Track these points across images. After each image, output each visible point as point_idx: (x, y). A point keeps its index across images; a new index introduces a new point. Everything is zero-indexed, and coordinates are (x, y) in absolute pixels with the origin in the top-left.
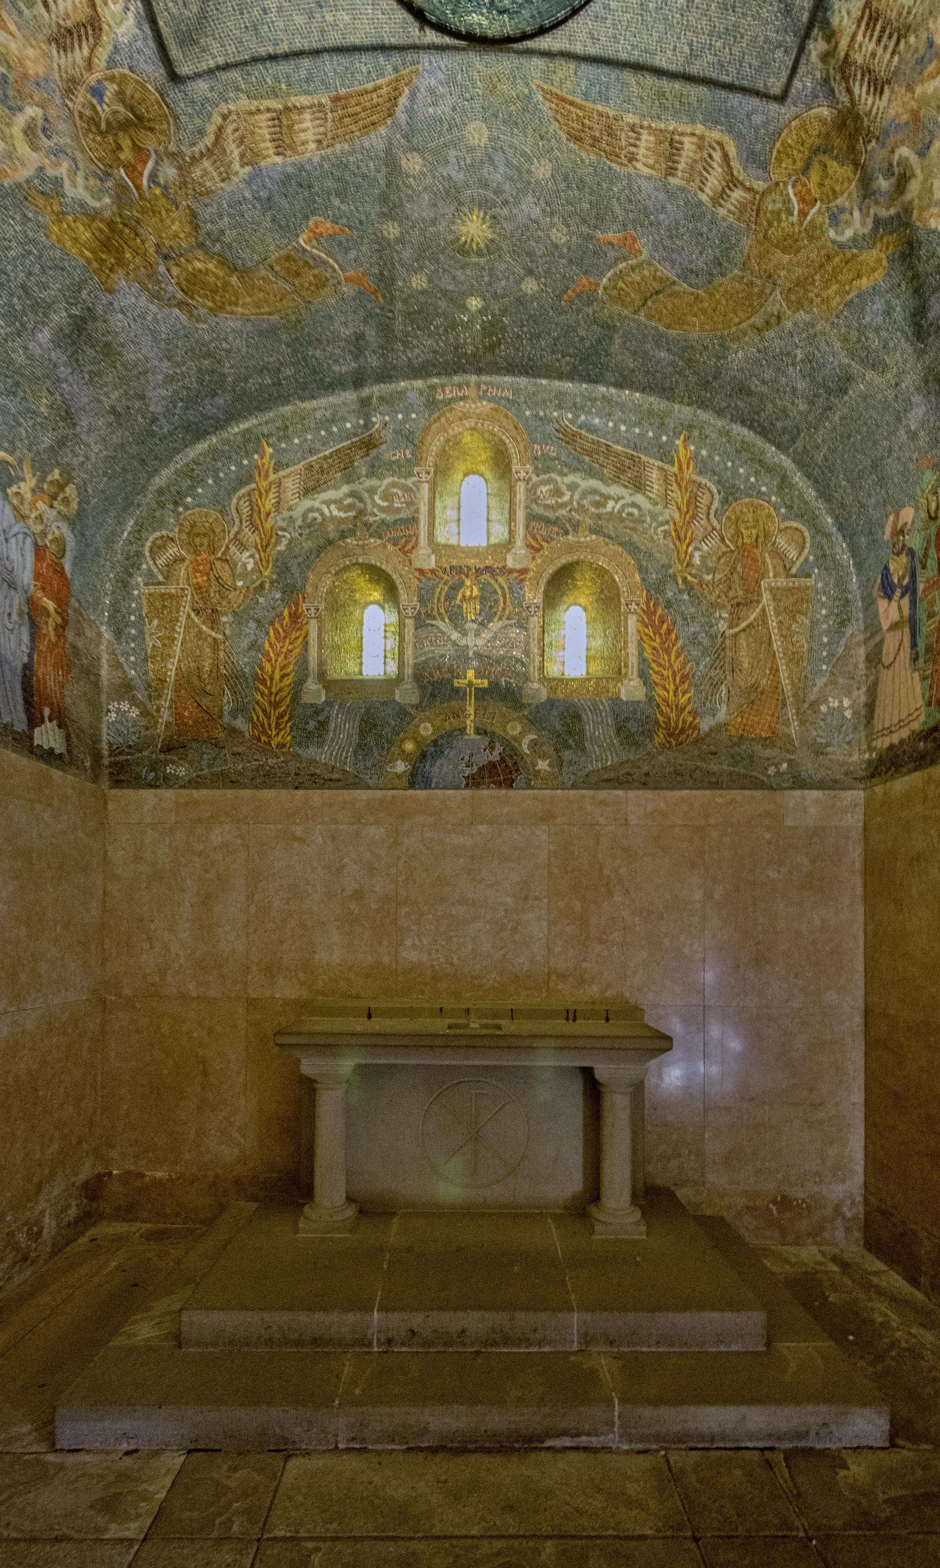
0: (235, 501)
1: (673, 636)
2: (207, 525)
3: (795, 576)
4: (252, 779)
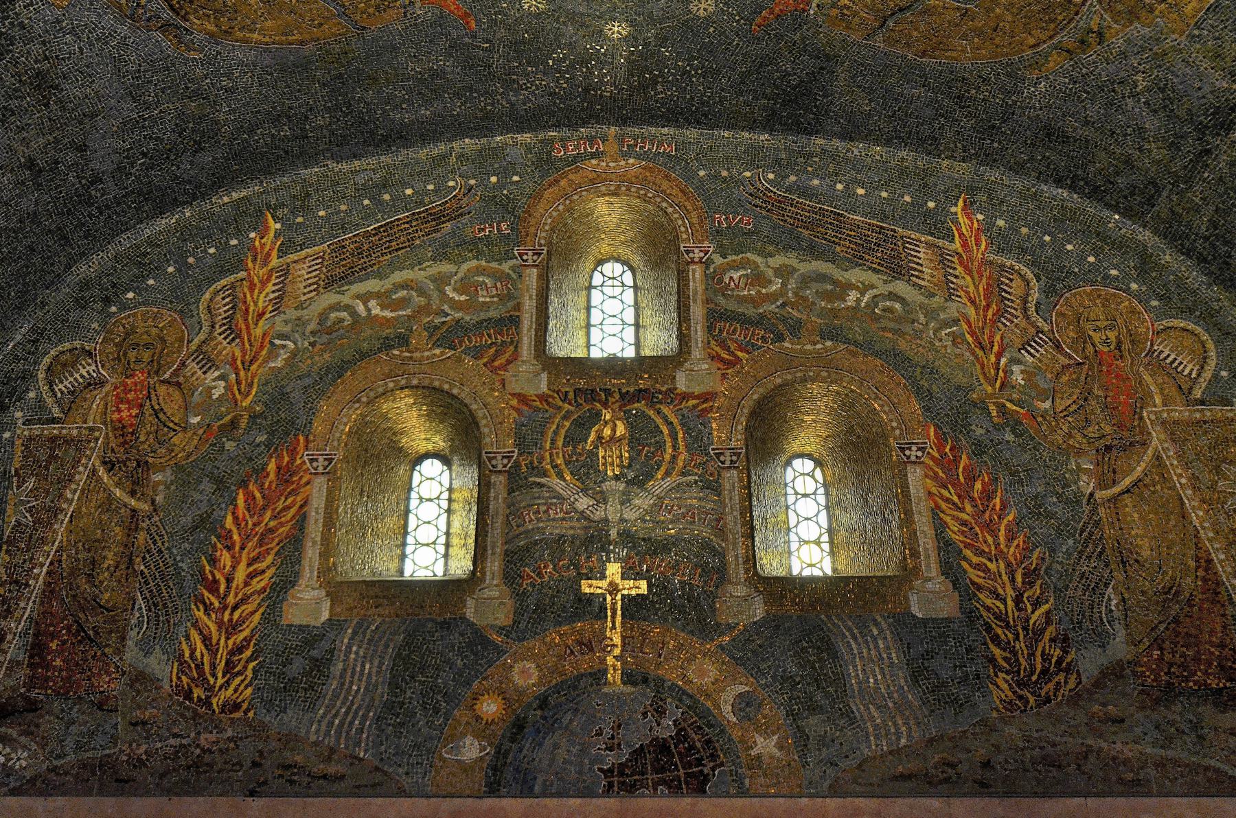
0: (207, 296)
2: (154, 331)
4: (162, 776)
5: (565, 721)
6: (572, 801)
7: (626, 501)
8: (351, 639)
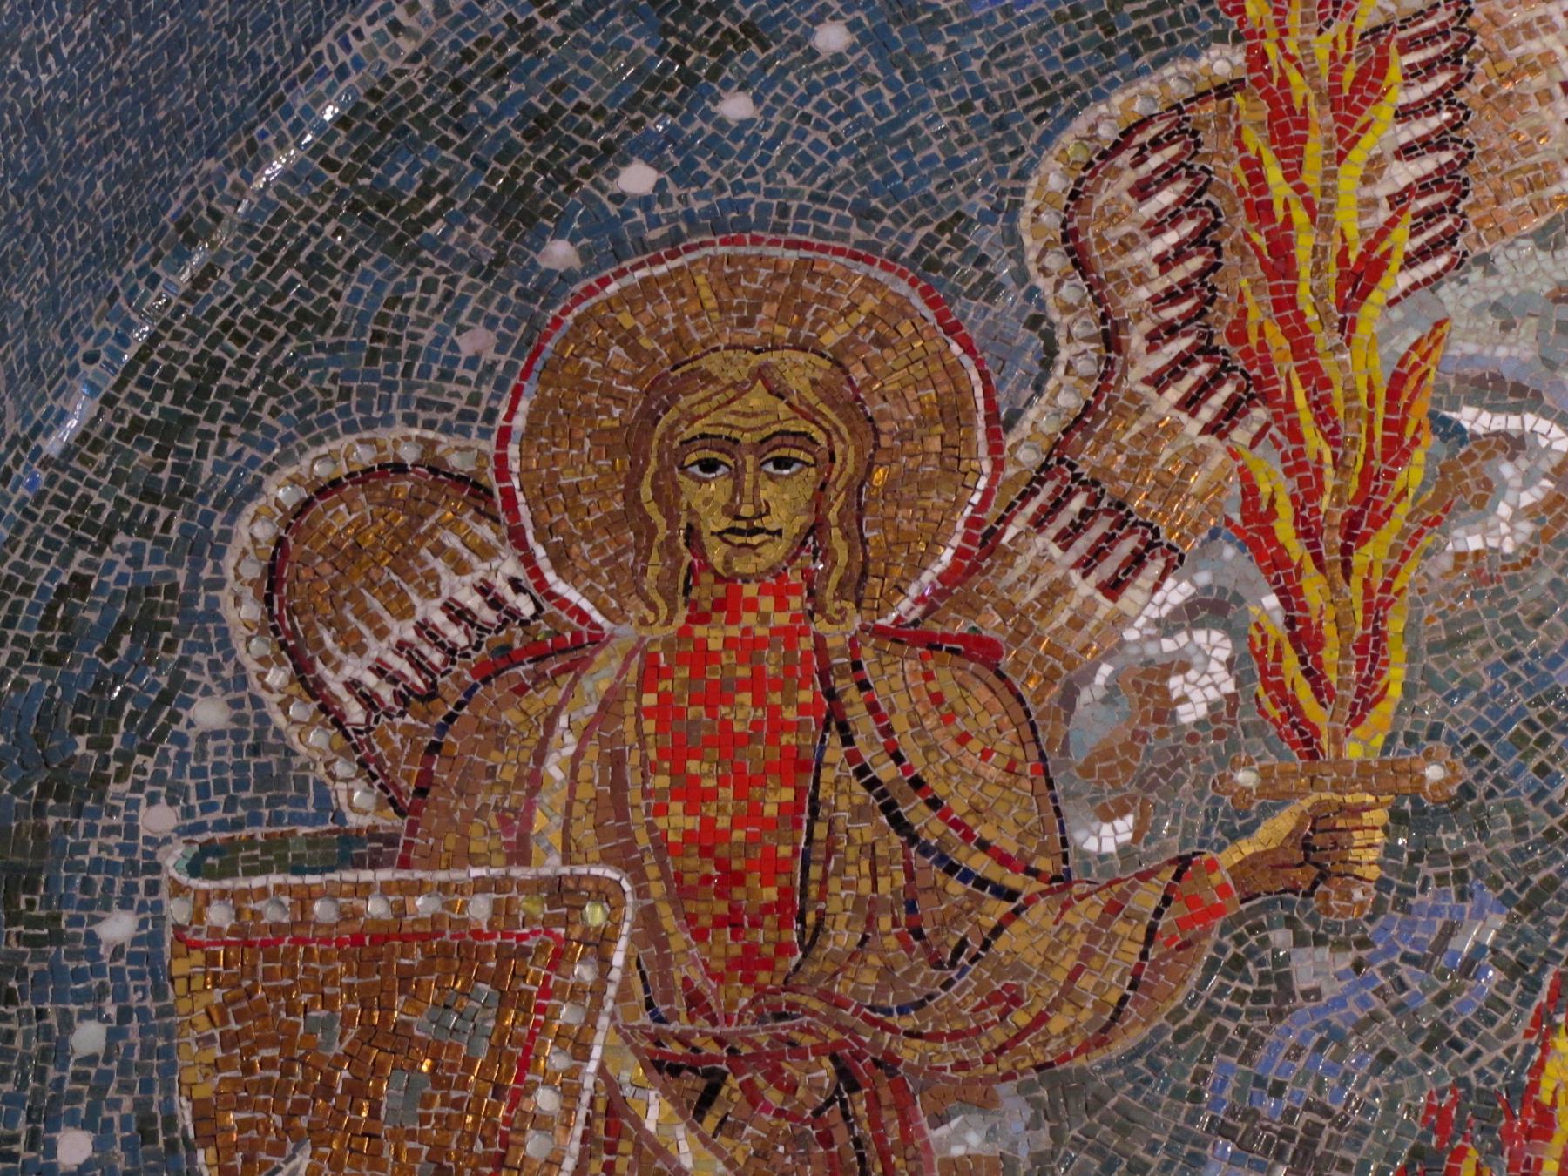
2: (799, 372)
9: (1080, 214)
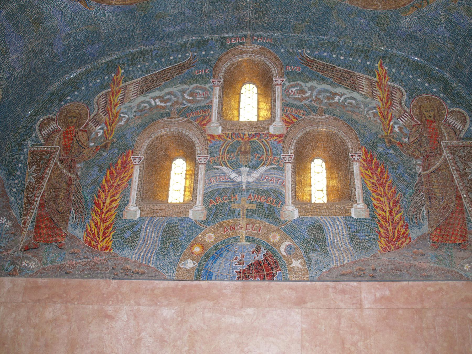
0: (97, 98)
1: (385, 175)
2: (77, 111)
3: (463, 139)
5: (224, 254)
6: (225, 282)
7: (249, 174)
8: (148, 224)
9: (99, 99)
